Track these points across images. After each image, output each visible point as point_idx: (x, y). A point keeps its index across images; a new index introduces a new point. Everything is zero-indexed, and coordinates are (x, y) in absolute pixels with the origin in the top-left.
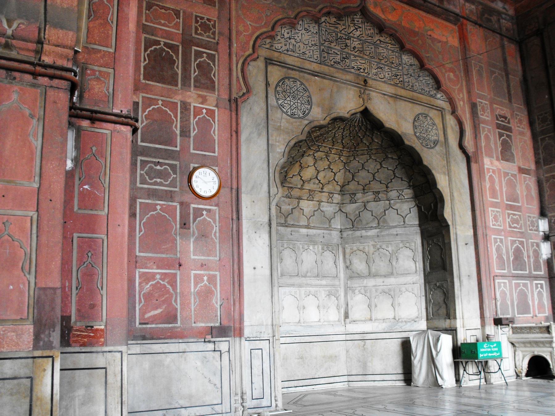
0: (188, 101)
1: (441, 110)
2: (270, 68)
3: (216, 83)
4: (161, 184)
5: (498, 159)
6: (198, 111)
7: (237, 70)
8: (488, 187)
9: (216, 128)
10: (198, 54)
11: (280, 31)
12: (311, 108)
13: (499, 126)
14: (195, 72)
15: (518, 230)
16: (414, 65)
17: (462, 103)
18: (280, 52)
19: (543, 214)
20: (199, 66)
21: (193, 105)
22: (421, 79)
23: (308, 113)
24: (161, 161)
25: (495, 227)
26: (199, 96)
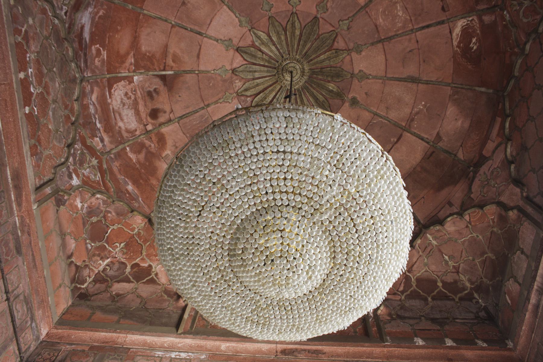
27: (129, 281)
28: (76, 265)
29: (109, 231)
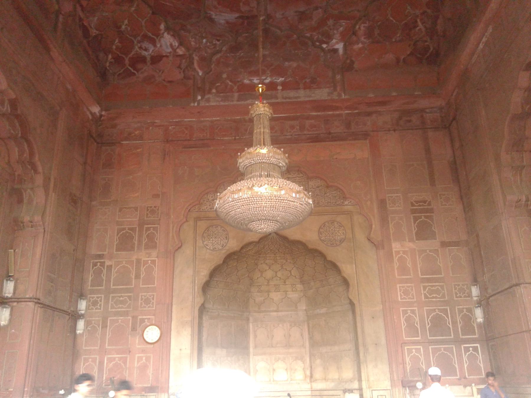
0: (140, 258)
1: (349, 213)
2: (199, 223)
3: (158, 243)
4: (122, 308)
5: (411, 240)
6: (146, 262)
7: (173, 231)
8: (396, 267)
9: (156, 270)
10: (148, 229)
11: (206, 197)
12: (228, 241)
13: (413, 212)
14: (145, 240)
15: (438, 300)
16: (321, 186)
17: (369, 203)
18: (206, 211)
19: (475, 281)
20: (148, 236)
21: (143, 259)
22: (328, 194)
23: (225, 246)
24: (123, 295)
25: (404, 300)
26: (147, 253)
27: (437, 17)
28: (409, 55)
29: (391, 19)
